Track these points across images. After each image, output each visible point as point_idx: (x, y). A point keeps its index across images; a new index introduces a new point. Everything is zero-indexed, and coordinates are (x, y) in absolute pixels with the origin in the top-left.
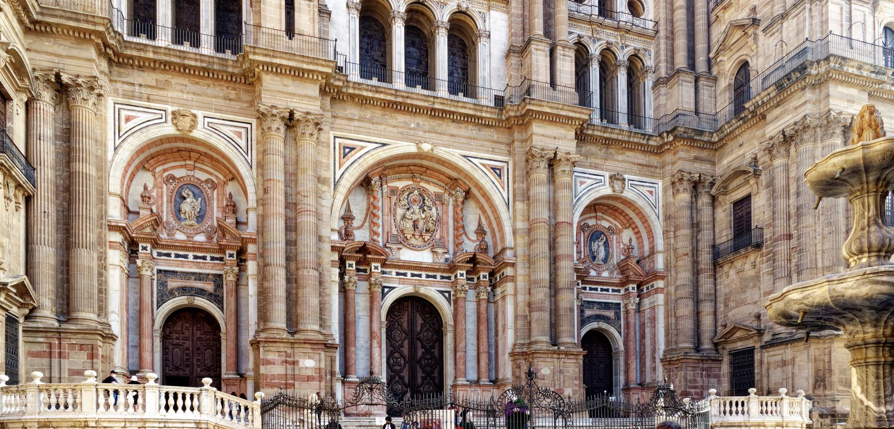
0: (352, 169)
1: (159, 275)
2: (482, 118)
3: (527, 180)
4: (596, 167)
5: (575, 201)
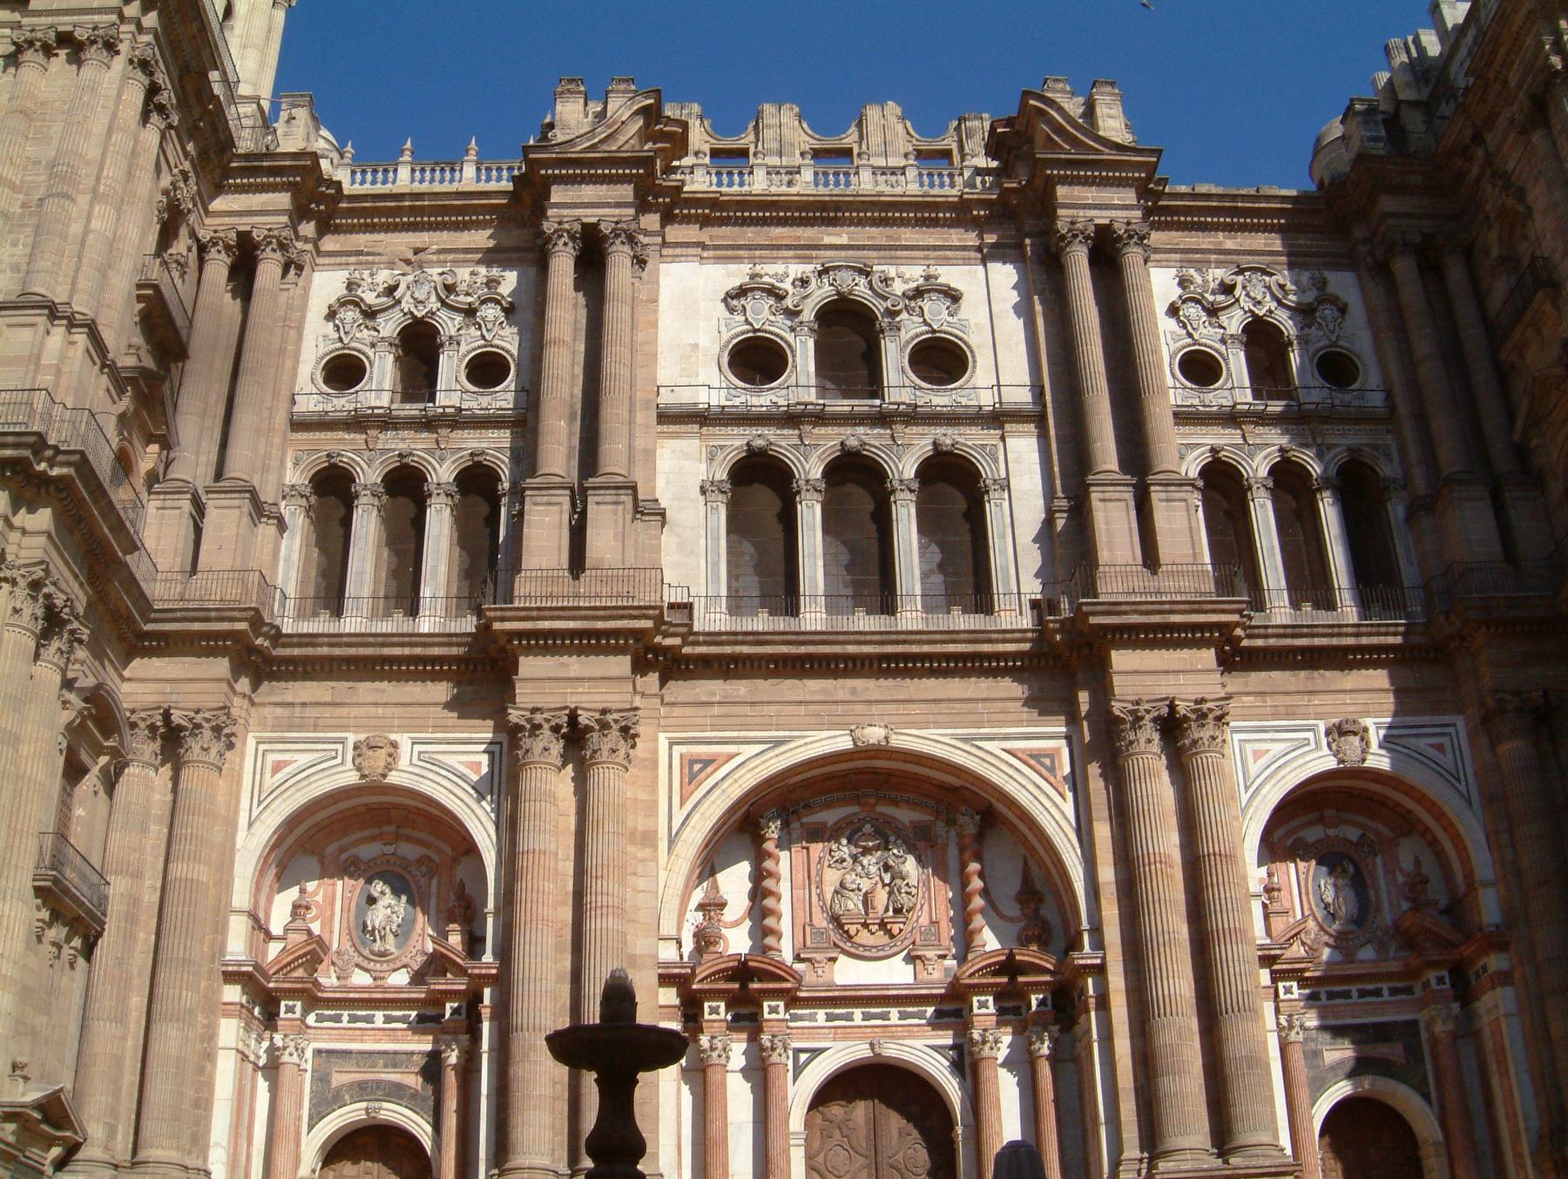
0: (707, 803)
1: (317, 1061)
4: (1289, 715)
5: (1245, 797)
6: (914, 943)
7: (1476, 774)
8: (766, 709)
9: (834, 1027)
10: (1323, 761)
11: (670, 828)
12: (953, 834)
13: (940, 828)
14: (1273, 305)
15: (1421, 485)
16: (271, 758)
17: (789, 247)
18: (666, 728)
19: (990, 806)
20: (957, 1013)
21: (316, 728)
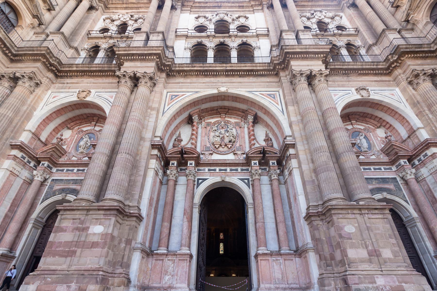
7: (407, 100)
8: (194, 84)
10: (356, 97)
11: (164, 111)
14: (324, 17)
15: (370, 41)
16: (54, 95)
17: (210, 11)
18: (165, 88)
21: (69, 88)
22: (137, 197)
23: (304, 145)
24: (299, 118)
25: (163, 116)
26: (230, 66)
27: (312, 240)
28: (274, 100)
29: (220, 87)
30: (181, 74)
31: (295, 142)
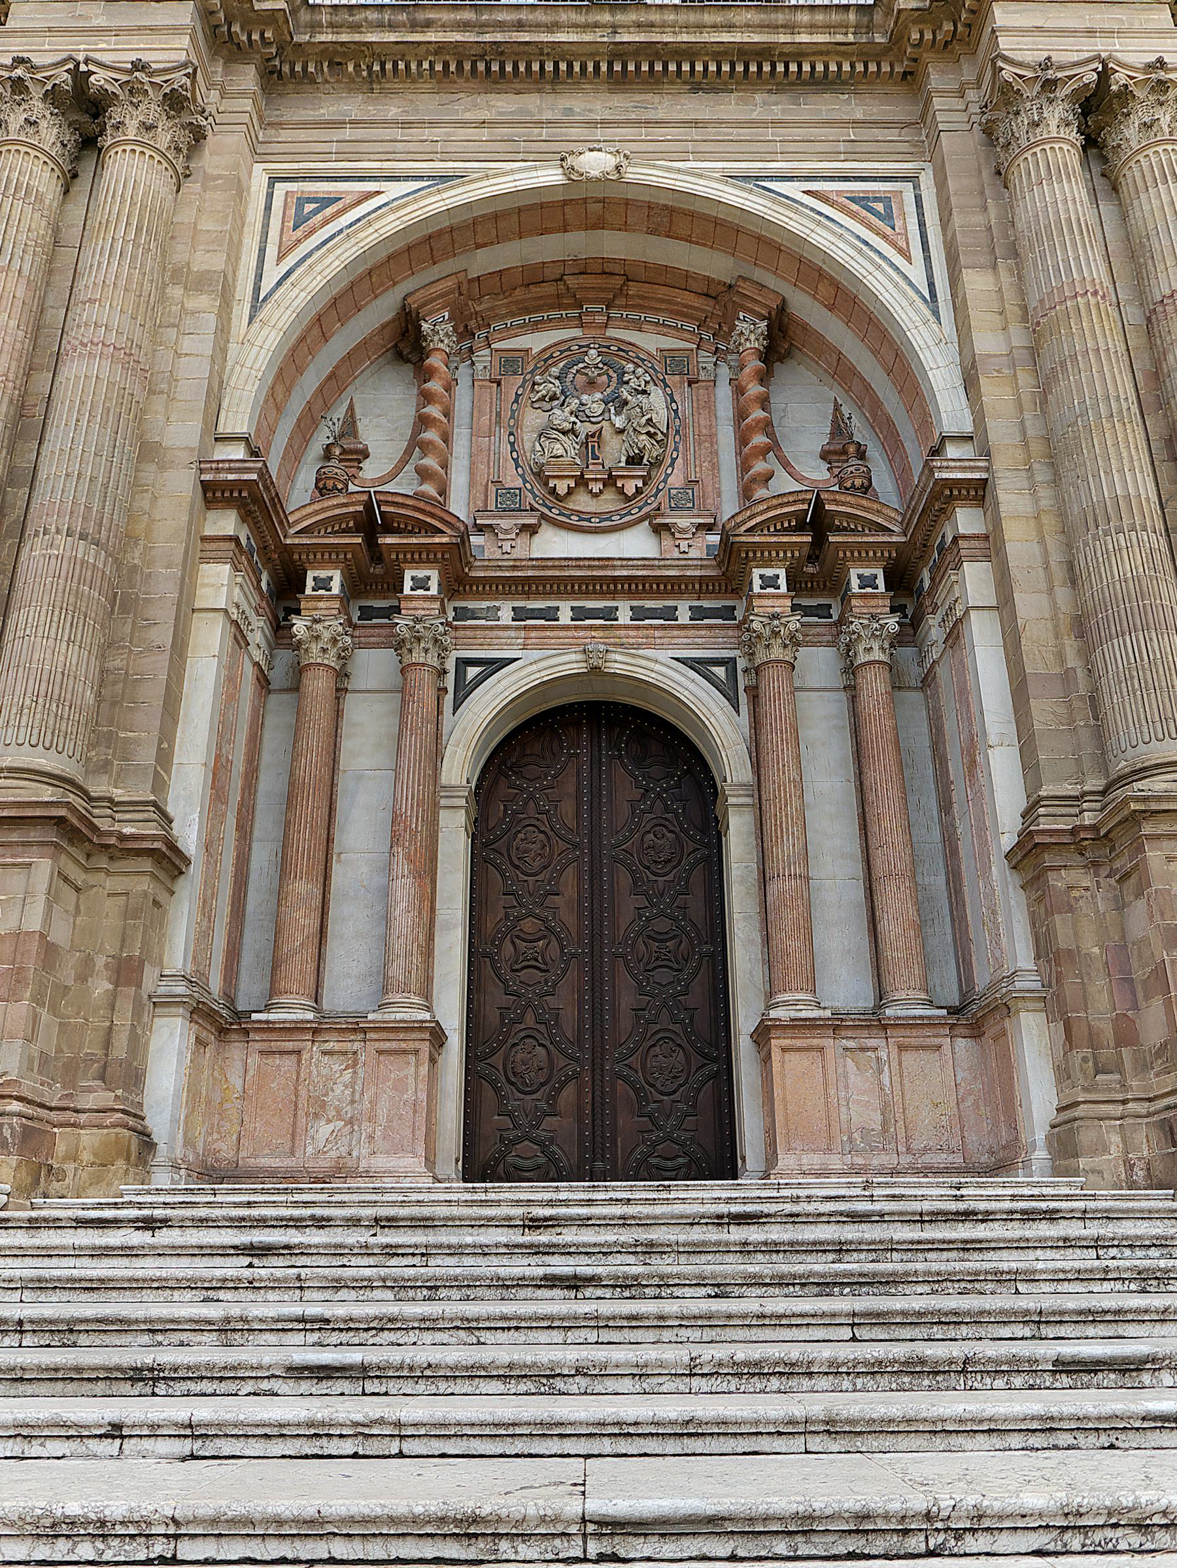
2: (799, 53)
3: (998, 197)
6: (659, 509)
8: (427, 133)
9: (525, 627)
11: (257, 289)
12: (724, 372)
13: (706, 358)
18: (258, 156)
19: (783, 308)
20: (728, 613)
22: (147, 756)
23: (1033, 488)
24: (1019, 337)
25: (256, 325)
26: (639, 26)
27: (1038, 957)
28: (889, 231)
29: (580, 147)
30: (351, 68)
31: (987, 469)
